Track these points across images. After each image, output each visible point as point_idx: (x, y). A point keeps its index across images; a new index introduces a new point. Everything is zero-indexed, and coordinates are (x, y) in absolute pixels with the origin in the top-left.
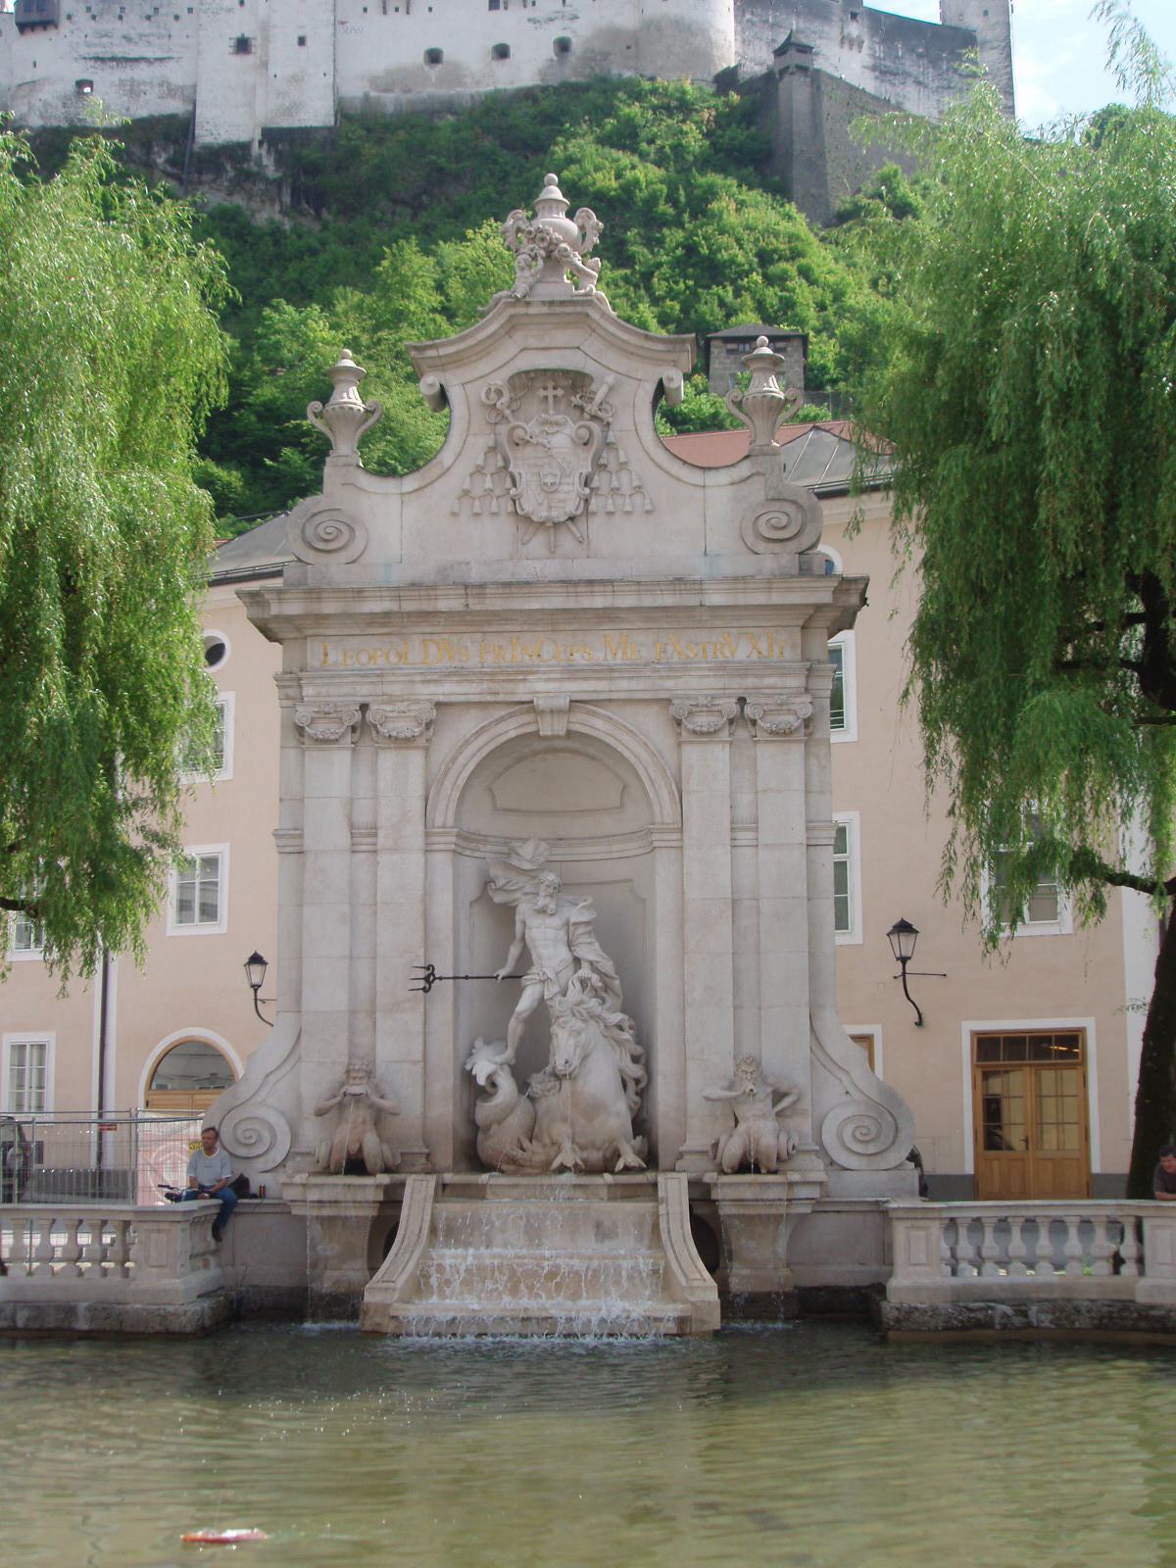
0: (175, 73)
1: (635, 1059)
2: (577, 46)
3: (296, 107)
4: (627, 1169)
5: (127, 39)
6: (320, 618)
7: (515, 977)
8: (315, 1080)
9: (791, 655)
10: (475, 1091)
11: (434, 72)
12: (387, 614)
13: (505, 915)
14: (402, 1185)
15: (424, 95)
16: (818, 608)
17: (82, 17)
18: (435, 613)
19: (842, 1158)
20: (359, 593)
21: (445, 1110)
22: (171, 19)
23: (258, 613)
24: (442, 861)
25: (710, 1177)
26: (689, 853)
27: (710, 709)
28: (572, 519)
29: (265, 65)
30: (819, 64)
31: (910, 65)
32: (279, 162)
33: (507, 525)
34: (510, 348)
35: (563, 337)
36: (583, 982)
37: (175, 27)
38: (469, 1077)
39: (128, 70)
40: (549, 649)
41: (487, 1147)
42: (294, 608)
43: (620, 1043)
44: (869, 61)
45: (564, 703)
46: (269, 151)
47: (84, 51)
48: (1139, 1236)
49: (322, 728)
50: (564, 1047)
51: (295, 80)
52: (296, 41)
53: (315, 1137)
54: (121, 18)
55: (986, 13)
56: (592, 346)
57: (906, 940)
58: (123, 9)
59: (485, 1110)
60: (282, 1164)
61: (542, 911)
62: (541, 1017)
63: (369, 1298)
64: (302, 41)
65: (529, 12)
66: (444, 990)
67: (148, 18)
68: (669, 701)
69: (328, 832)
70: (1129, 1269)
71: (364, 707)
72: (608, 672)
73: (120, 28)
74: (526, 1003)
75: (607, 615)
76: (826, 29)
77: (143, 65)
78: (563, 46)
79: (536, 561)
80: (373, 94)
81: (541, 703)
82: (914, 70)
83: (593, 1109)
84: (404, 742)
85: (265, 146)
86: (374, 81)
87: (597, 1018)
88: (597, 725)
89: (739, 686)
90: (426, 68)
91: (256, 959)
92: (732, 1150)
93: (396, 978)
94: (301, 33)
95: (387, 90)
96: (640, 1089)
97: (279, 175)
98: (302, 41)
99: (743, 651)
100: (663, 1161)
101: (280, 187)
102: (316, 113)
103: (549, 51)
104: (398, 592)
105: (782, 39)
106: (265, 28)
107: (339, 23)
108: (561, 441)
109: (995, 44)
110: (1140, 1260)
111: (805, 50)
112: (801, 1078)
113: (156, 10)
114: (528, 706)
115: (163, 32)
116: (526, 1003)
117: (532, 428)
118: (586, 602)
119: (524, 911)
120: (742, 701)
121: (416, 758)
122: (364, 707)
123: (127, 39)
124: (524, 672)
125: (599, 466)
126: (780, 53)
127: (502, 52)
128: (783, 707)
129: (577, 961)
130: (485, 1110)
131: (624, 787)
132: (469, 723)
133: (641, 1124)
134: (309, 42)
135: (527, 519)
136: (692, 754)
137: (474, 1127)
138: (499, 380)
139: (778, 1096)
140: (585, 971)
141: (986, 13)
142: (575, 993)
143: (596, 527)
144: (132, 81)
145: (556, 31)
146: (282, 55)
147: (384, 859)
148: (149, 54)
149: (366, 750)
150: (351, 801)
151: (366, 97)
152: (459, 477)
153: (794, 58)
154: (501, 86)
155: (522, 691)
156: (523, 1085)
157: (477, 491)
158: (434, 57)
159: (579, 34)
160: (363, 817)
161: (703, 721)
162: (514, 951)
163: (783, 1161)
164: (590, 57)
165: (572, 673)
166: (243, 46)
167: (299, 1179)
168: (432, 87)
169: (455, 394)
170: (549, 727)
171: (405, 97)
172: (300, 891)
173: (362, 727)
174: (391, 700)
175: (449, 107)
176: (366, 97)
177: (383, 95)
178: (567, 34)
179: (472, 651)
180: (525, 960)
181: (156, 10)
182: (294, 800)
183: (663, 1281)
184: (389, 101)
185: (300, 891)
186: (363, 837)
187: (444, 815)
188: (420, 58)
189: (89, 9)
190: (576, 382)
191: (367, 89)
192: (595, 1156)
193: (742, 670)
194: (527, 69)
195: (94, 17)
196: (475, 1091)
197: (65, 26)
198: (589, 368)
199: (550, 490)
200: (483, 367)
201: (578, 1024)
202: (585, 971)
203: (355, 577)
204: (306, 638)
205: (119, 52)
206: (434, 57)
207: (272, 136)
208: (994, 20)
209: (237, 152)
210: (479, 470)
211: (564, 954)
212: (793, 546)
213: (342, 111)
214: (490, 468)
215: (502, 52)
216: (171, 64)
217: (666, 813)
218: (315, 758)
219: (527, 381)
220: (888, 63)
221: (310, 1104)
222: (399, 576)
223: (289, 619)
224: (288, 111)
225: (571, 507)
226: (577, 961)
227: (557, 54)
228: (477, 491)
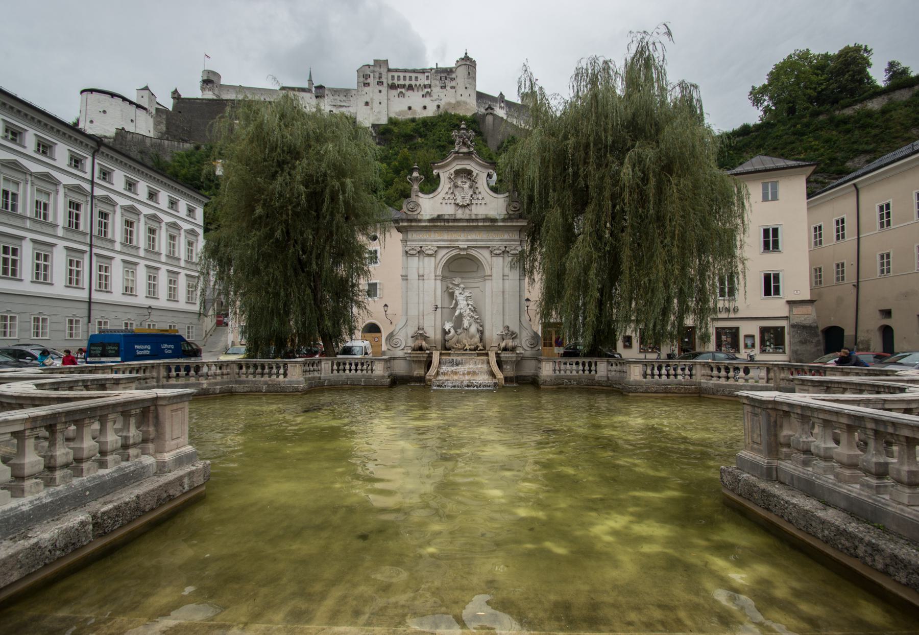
0: (352, 110)
1: (481, 326)
2: (441, 107)
3: (379, 119)
4: (480, 350)
6: (411, 227)
7: (455, 308)
8: (411, 330)
9: (517, 237)
10: (445, 333)
11: (410, 112)
12: (426, 226)
13: (452, 295)
14: (432, 353)
16: (523, 226)
17: (330, 95)
18: (437, 226)
19: (526, 348)
20: (420, 221)
21: (439, 336)
23: (396, 225)
24: (439, 283)
25: (499, 352)
26: (494, 281)
27: (498, 249)
28: (468, 205)
29: (372, 109)
30: (495, 113)
32: (375, 132)
33: (453, 206)
34: (454, 164)
35: (466, 162)
36: (470, 309)
37: (351, 99)
38: (444, 330)
40: (462, 236)
41: (448, 345)
42: (405, 224)
43: (478, 323)
45: (466, 246)
48: (596, 365)
49: (411, 252)
50: (466, 323)
51: (379, 112)
53: (411, 343)
56: (473, 164)
57: (528, 303)
59: (447, 337)
60: (403, 349)
61: (460, 294)
62: (461, 316)
63: (427, 377)
64: (380, 103)
65: (431, 98)
66: (439, 310)
68: (489, 247)
69: (413, 276)
70: (593, 373)
71: (421, 247)
72: (476, 240)
74: (457, 313)
75: (477, 227)
78: (438, 107)
79: (460, 214)
81: (461, 246)
83: (472, 337)
84: (430, 255)
86: (396, 113)
87: (473, 317)
88: (473, 252)
89: (505, 243)
91: (386, 305)
92: (503, 345)
93: (429, 308)
96: (481, 332)
98: (380, 103)
99: (506, 237)
100: (487, 348)
102: (384, 121)
103: (435, 108)
104: (430, 220)
105: (487, 106)
106: (372, 99)
107: (388, 99)
108: (466, 186)
110: (596, 371)
111: (492, 109)
112: (517, 330)
114: (458, 247)
116: (457, 313)
117: (459, 183)
118: (471, 224)
119: (457, 293)
120: (506, 247)
121: (433, 259)
122: (421, 247)
124: (457, 240)
125: (475, 193)
126: (486, 109)
127: (425, 108)
128: (515, 249)
129: (468, 305)
130: (447, 337)
131: (478, 267)
132: (444, 252)
133: (481, 340)
135: (458, 205)
136: (494, 259)
137: (445, 341)
138: (452, 171)
139: (513, 333)
140: (470, 307)
142: (468, 311)
143: (473, 207)
145: (437, 103)
146: (376, 105)
147: (426, 281)
148: (345, 104)
149: (421, 257)
150: (418, 268)
152: (442, 195)
153: (490, 111)
155: (456, 244)
156: (456, 332)
157: (447, 198)
158: (410, 108)
159: (442, 104)
160: (421, 273)
161: (497, 252)
162: (454, 302)
163: (513, 349)
165: (468, 240)
166: (367, 104)
167: (409, 351)
168: (409, 116)
169: (441, 175)
170: (462, 253)
172: (407, 288)
173: (421, 252)
174: (427, 246)
175: (413, 120)
179: (446, 236)
180: (456, 304)
182: (406, 268)
183: (492, 374)
185: (407, 288)
186: (421, 277)
187: (439, 272)
188: (407, 109)
190: (469, 173)
192: (472, 347)
193: (506, 240)
194: (431, 112)
196: (445, 333)
197: (326, 97)
198: (472, 169)
199: (463, 198)
200: (447, 169)
201: (468, 318)
202: (470, 307)
203: (419, 217)
204: (407, 231)
205: (339, 103)
206: (410, 108)
207: (374, 126)
210: (447, 193)
211: (465, 302)
212: (517, 213)
213: (391, 120)
214: (450, 192)
215: (425, 108)
217: (488, 272)
218: (410, 259)
219: (458, 173)
221: (410, 336)
222: (428, 217)
223: (404, 226)
225: (468, 202)
226: (468, 305)
228: (447, 198)
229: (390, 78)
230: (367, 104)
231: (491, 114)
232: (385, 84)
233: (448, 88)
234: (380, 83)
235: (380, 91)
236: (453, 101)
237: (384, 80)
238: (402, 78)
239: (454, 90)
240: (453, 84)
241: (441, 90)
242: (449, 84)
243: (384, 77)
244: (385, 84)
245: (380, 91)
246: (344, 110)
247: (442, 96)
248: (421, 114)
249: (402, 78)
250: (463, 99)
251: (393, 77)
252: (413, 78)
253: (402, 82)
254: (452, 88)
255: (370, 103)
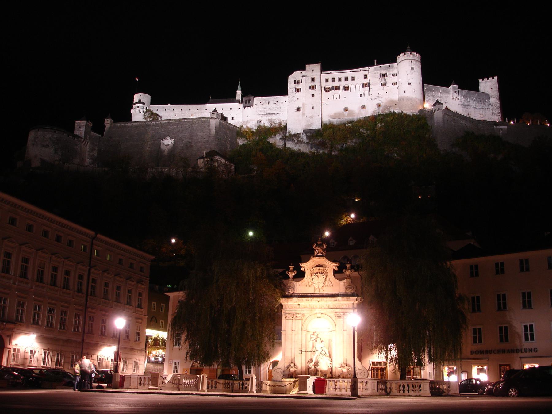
3: (312, 124)
5: (270, 109)
11: (346, 113)
15: (344, 119)
22: (281, 103)
31: (471, 103)
39: (270, 117)
44: (461, 103)
46: (305, 135)
47: (260, 113)
51: (311, 117)
52: (312, 108)
54: (268, 104)
55: (492, 88)
58: (269, 102)
64: (313, 108)
67: (275, 103)
73: (268, 106)
76: (448, 95)
77: (274, 115)
78: (379, 105)
80: (331, 119)
82: (473, 104)
85: (304, 134)
86: (331, 116)
90: (344, 112)
94: (313, 106)
95: (334, 119)
97: (308, 141)
98: (313, 108)
101: (308, 145)
102: (317, 125)
109: (494, 96)
113: (277, 102)
115: (279, 107)
123: (270, 109)
127: (363, 107)
134: (314, 108)
141: (492, 88)
144: (271, 119)
145: (377, 101)
146: (308, 111)
151: (329, 121)
153: (437, 106)
154: (364, 116)
158: (346, 109)
159: (383, 102)
164: (386, 108)
166: (298, 109)
168: (346, 117)
171: (339, 120)
176: (329, 121)
177: (334, 119)
178: (380, 102)
181: (277, 102)
184: (335, 121)
188: (343, 110)
189: (261, 102)
191: (329, 118)
194: (370, 111)
195: (262, 104)
207: (306, 132)
208: (494, 90)
209: (297, 136)
216: (281, 114)
220: (465, 103)
224: (310, 125)
227: (377, 107)
229: (323, 80)
230: (298, 109)
231: (439, 109)
232: (318, 88)
233: (389, 84)
234: (313, 88)
235: (313, 96)
236: (396, 98)
237: (317, 83)
238: (337, 79)
239: (396, 86)
240: (395, 79)
241: (382, 87)
242: (389, 79)
243: (317, 80)
244: (318, 88)
245: (313, 96)
246: (273, 117)
247: (383, 93)
248: (358, 114)
249: (337, 79)
250: (406, 95)
251: (327, 80)
252: (350, 79)
253: (337, 83)
254: (394, 84)
255: (301, 109)
